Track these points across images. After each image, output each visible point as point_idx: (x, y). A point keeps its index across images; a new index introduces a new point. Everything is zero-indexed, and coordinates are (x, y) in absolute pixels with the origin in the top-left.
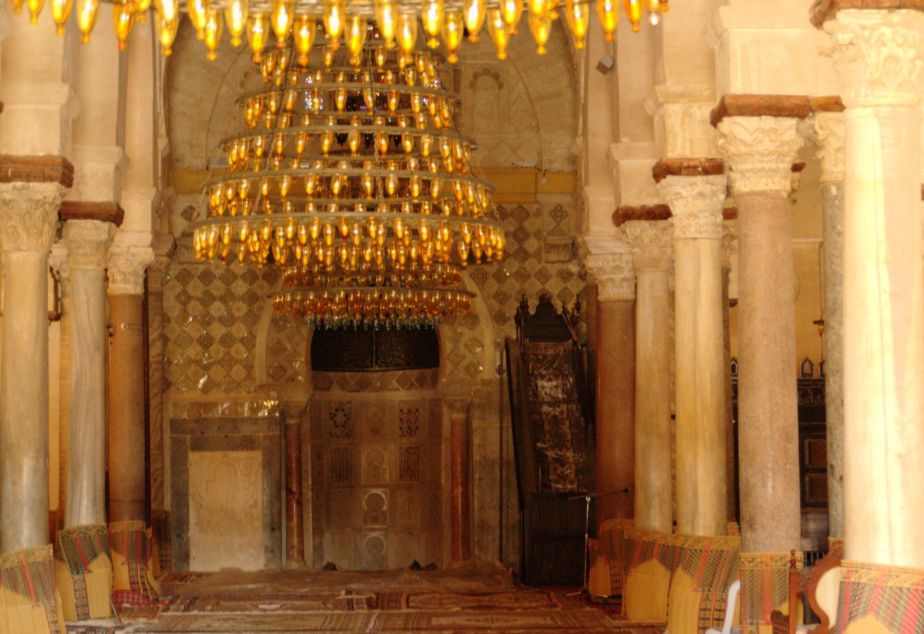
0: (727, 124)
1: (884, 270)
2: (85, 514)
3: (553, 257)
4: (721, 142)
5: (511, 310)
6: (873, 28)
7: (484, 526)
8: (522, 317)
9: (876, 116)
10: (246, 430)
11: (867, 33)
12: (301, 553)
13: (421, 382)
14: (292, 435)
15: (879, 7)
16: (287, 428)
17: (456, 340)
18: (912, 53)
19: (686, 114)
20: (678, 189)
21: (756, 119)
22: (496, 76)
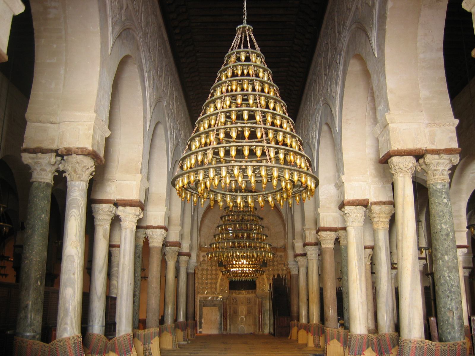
0: (319, 233)
1: (356, 262)
2: (181, 319)
3: (280, 266)
4: (319, 237)
5: (271, 277)
6: (352, 210)
7: (265, 324)
8: (274, 279)
9: (354, 228)
10: (215, 302)
11: (351, 211)
12: (226, 329)
13: (252, 292)
14: (225, 304)
15: (353, 205)
16: (223, 302)
17: (260, 283)
18: (361, 215)
19: (310, 233)
20: (309, 249)
21: (326, 232)
22: (268, 228)
